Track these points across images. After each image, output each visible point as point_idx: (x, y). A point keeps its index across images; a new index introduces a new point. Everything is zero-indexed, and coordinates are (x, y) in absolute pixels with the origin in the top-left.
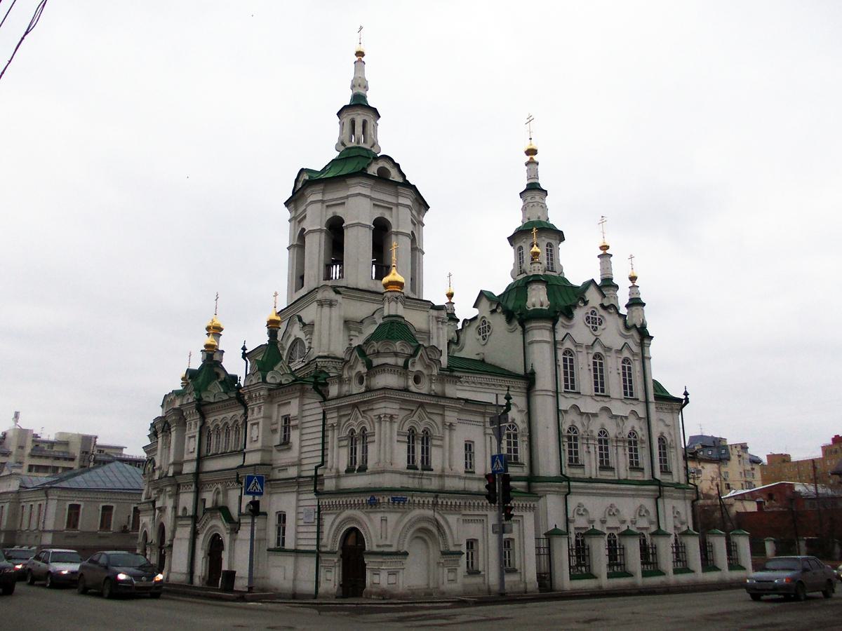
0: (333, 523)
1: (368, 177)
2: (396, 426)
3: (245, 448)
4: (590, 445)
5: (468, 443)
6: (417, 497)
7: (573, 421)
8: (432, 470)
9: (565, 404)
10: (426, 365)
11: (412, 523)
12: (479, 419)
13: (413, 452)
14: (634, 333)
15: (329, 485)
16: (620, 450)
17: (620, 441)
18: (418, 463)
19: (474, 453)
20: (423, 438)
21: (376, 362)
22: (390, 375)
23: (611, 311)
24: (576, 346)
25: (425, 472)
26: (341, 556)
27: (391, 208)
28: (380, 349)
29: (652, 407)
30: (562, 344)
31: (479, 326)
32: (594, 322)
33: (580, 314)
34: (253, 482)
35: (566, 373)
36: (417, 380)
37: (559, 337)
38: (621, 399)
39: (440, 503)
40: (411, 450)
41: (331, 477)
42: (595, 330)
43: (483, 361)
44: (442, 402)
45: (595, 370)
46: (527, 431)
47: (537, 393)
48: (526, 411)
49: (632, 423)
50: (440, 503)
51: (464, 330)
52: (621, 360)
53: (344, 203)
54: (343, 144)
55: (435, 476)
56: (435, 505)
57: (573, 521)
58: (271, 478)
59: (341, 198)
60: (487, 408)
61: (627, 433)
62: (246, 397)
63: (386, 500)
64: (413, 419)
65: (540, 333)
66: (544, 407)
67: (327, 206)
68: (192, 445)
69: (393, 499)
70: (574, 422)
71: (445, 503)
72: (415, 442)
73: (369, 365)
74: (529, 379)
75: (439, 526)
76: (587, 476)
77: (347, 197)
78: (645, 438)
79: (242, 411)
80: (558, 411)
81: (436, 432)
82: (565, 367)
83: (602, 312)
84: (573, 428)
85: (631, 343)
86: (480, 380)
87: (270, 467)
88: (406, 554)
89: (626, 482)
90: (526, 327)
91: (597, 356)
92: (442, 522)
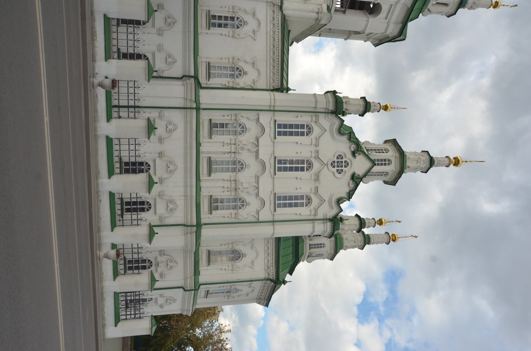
9: (266, 119)
17: (236, 183)
38: (274, 190)
42: (332, 164)
46: (238, 87)
48: (254, 88)
49: (254, 204)
57: (160, 117)
61: (243, 195)
70: (249, 131)
76: (201, 140)
78: (241, 219)
82: (297, 126)
83: (348, 172)
84: (244, 129)
85: (325, 206)
86: (276, 38)
89: (198, 189)
91: (310, 165)
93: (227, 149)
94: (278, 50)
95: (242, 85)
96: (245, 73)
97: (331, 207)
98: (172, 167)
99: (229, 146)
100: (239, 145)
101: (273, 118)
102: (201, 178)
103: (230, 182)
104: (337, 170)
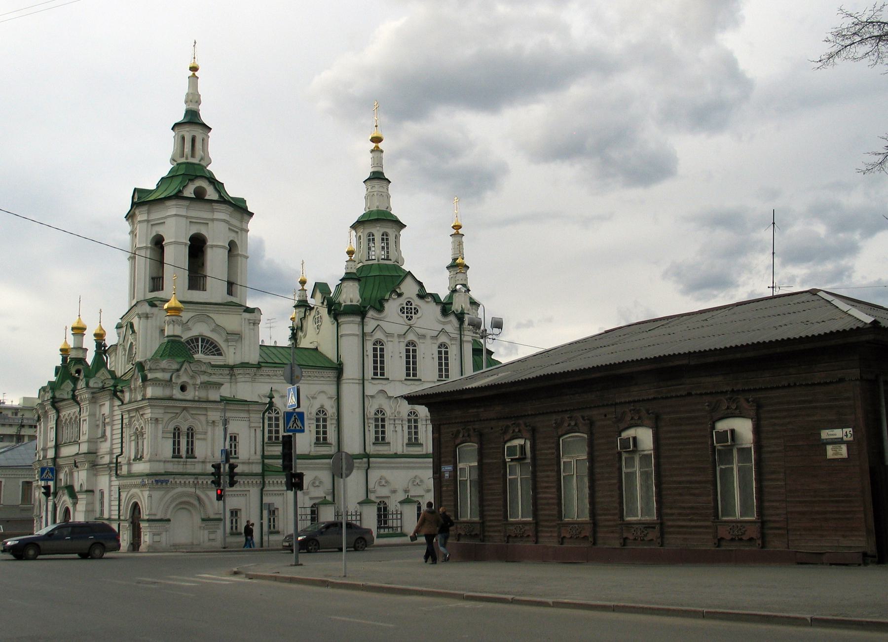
0: (126, 497)
1: (183, 199)
2: (160, 426)
3: (79, 439)
4: (396, 425)
5: (233, 435)
6: (178, 479)
7: (380, 405)
8: (196, 458)
9: (371, 389)
10: (191, 376)
11: (173, 499)
12: (245, 415)
13: (179, 444)
14: (453, 319)
15: (124, 470)
18: (183, 452)
19: (238, 442)
20: (188, 434)
21: (150, 376)
22: (158, 388)
23: (427, 300)
24: (387, 336)
25: (188, 460)
26: (132, 523)
27: (208, 223)
28: (151, 366)
31: (315, 316)
32: (409, 311)
33: (392, 307)
34: (46, 471)
35: (375, 362)
36: (183, 388)
37: (368, 329)
39: (200, 482)
40: (176, 444)
41: (125, 464)
42: (409, 320)
43: (316, 349)
44: (204, 405)
45: (408, 357)
47: (344, 381)
48: (336, 397)
50: (200, 482)
51: (306, 318)
52: (436, 346)
53: (164, 222)
54: (174, 160)
55: (199, 462)
56: (195, 485)
58: (96, 463)
59: (162, 218)
60: (250, 406)
62: (79, 399)
63: (150, 482)
64: (178, 419)
65: (350, 326)
66: (351, 393)
67: (152, 225)
68: (52, 435)
69: (157, 481)
70: (382, 406)
71: (205, 482)
72: (181, 437)
73: (145, 379)
74: (338, 369)
75: (199, 499)
76: (392, 452)
77: (166, 218)
79: (78, 409)
81: (199, 428)
82: (375, 356)
83: (417, 302)
84: (380, 411)
87: (95, 455)
88: (169, 520)
90: (339, 321)
92: (202, 496)
93: (399, 428)
95: (334, 410)
96: (322, 407)
97: (450, 322)
98: (418, 481)
99: (396, 425)
100: (395, 416)
101: (369, 381)
102: (424, 452)
104: (415, 313)
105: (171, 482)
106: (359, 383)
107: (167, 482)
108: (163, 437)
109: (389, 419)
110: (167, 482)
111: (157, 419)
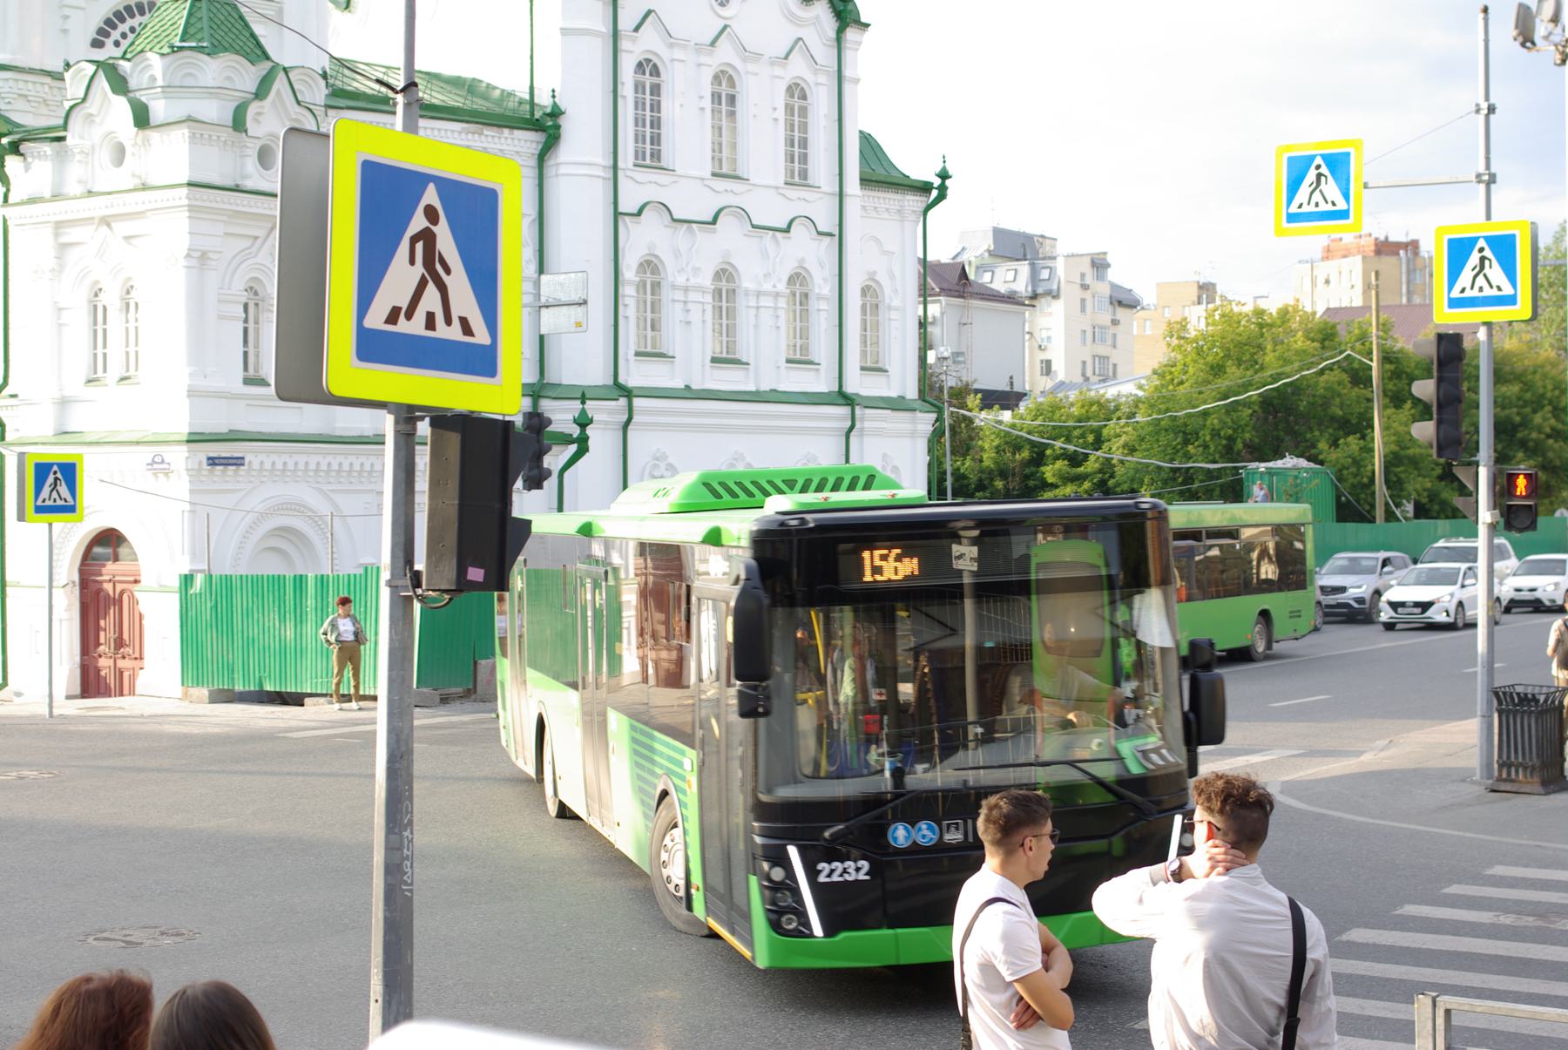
4: (690, 306)
16: (766, 317)
24: (671, 46)
29: (851, 207)
30: (634, 40)
38: (777, 188)
47: (563, 170)
52: (781, 88)
76: (679, 384)
80: (617, 215)
94: (446, 130)
99: (690, 306)
103: (762, 310)
105: (250, 463)
106: (604, 178)
107: (237, 462)
108: (221, 317)
109: (674, 287)
110: (237, 462)
111: (204, 257)
